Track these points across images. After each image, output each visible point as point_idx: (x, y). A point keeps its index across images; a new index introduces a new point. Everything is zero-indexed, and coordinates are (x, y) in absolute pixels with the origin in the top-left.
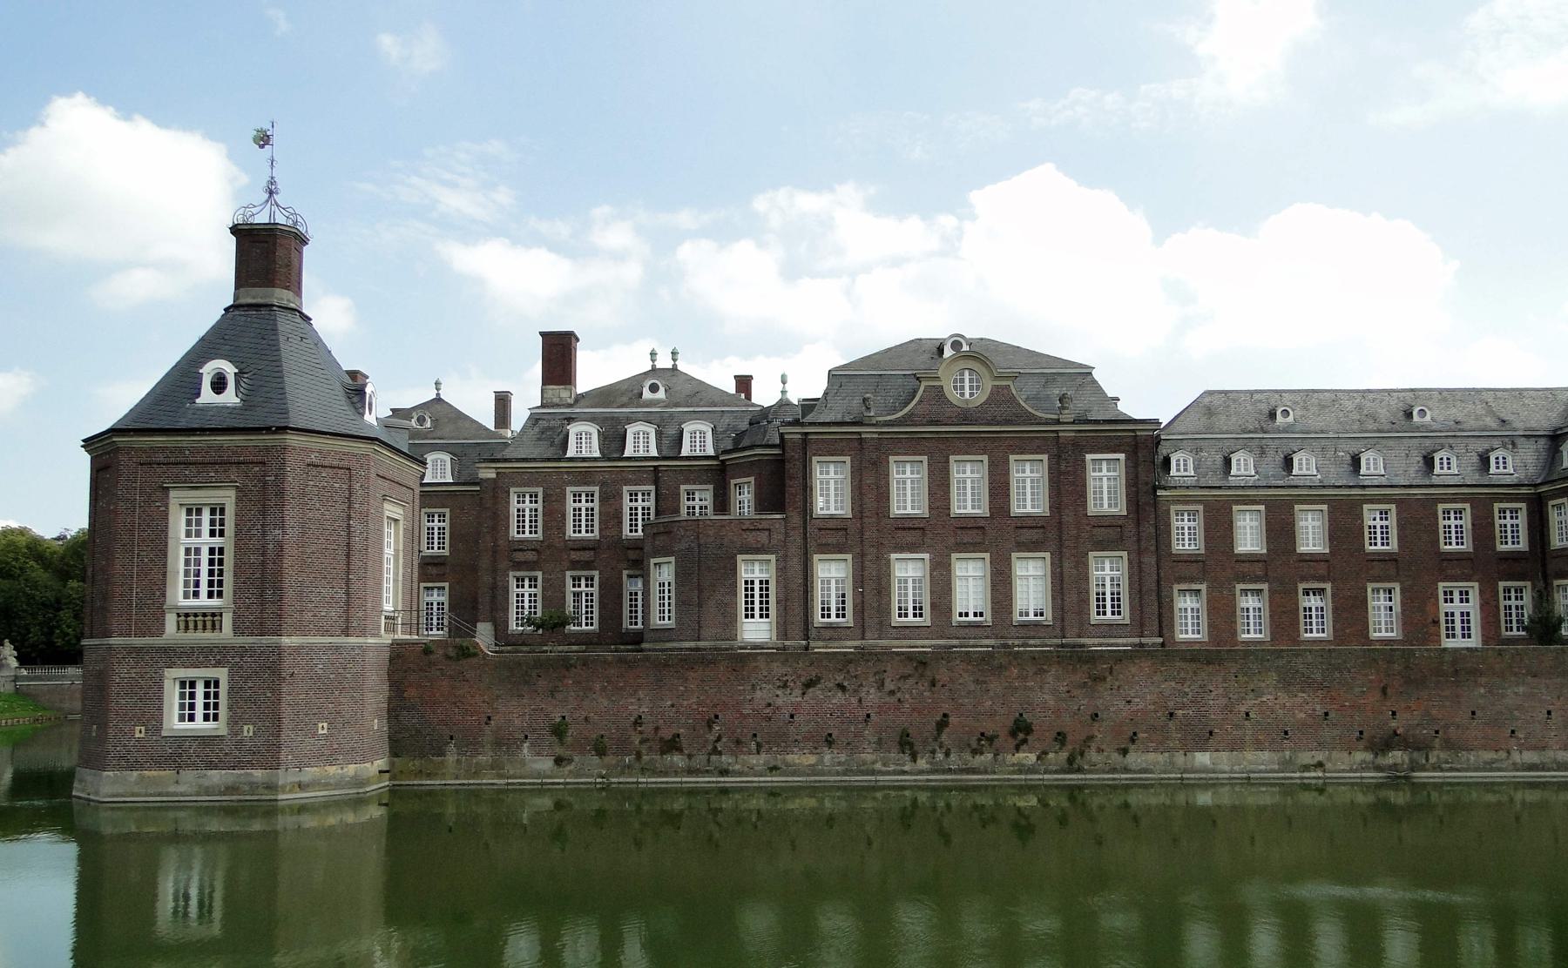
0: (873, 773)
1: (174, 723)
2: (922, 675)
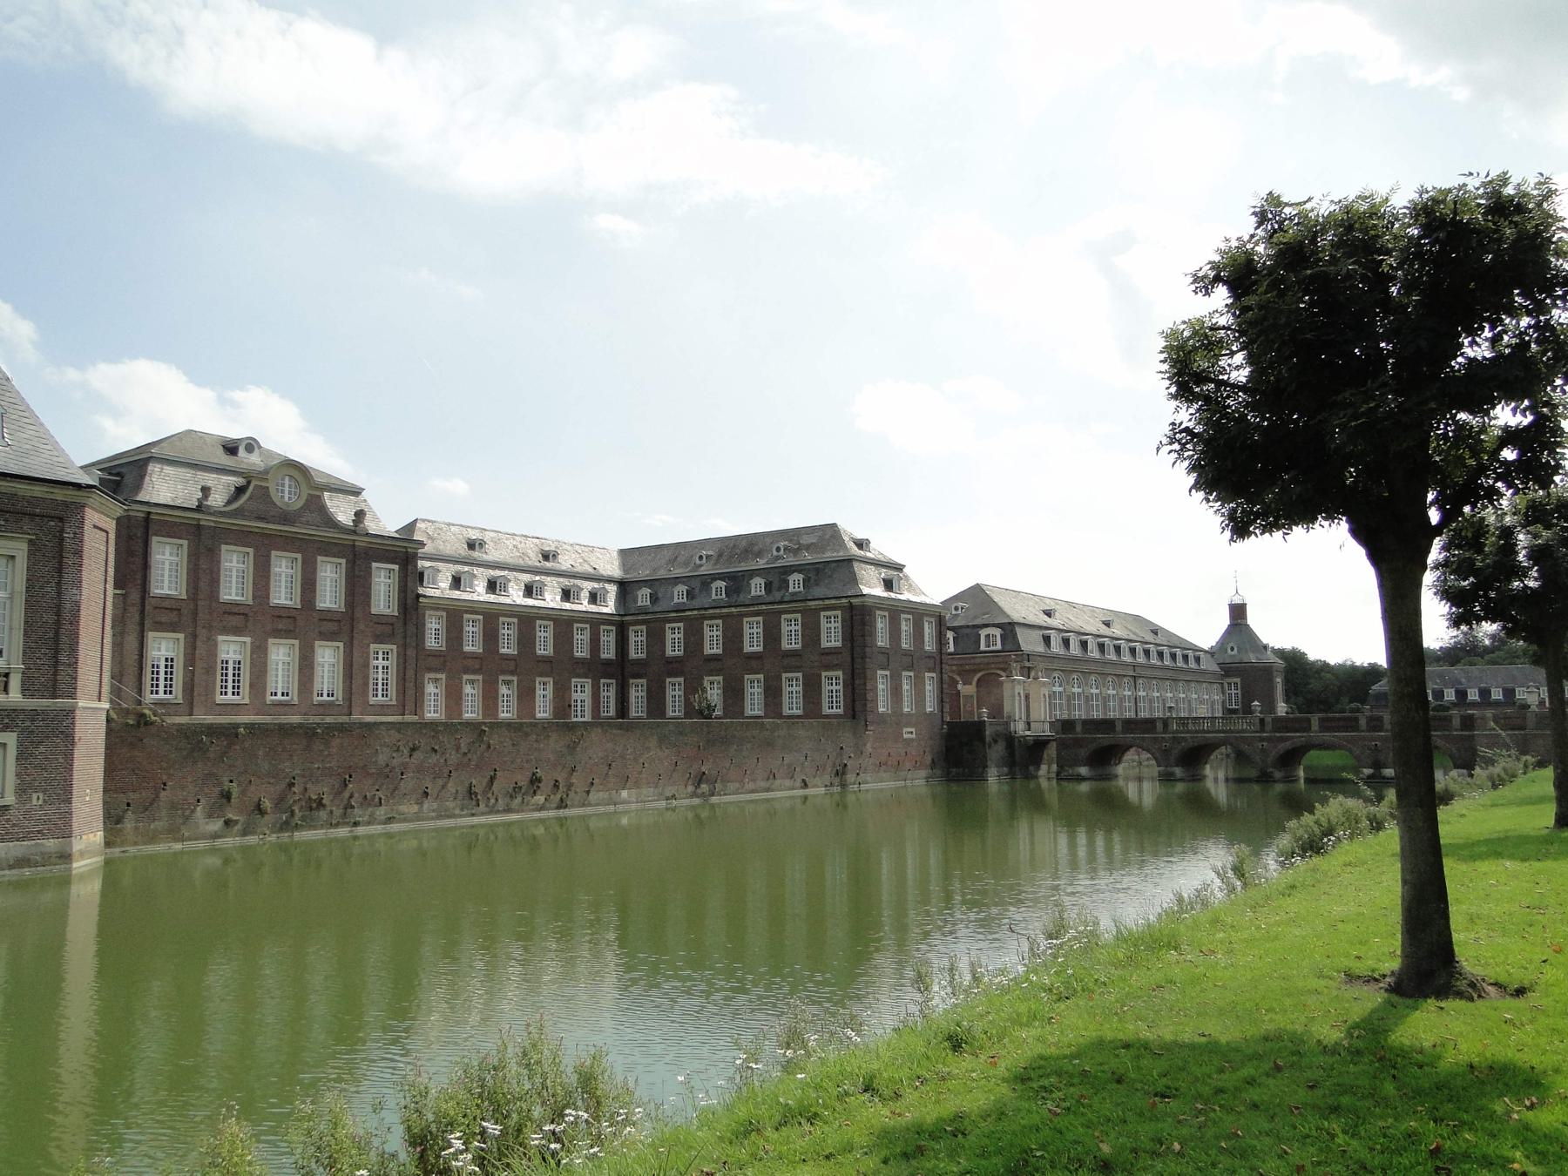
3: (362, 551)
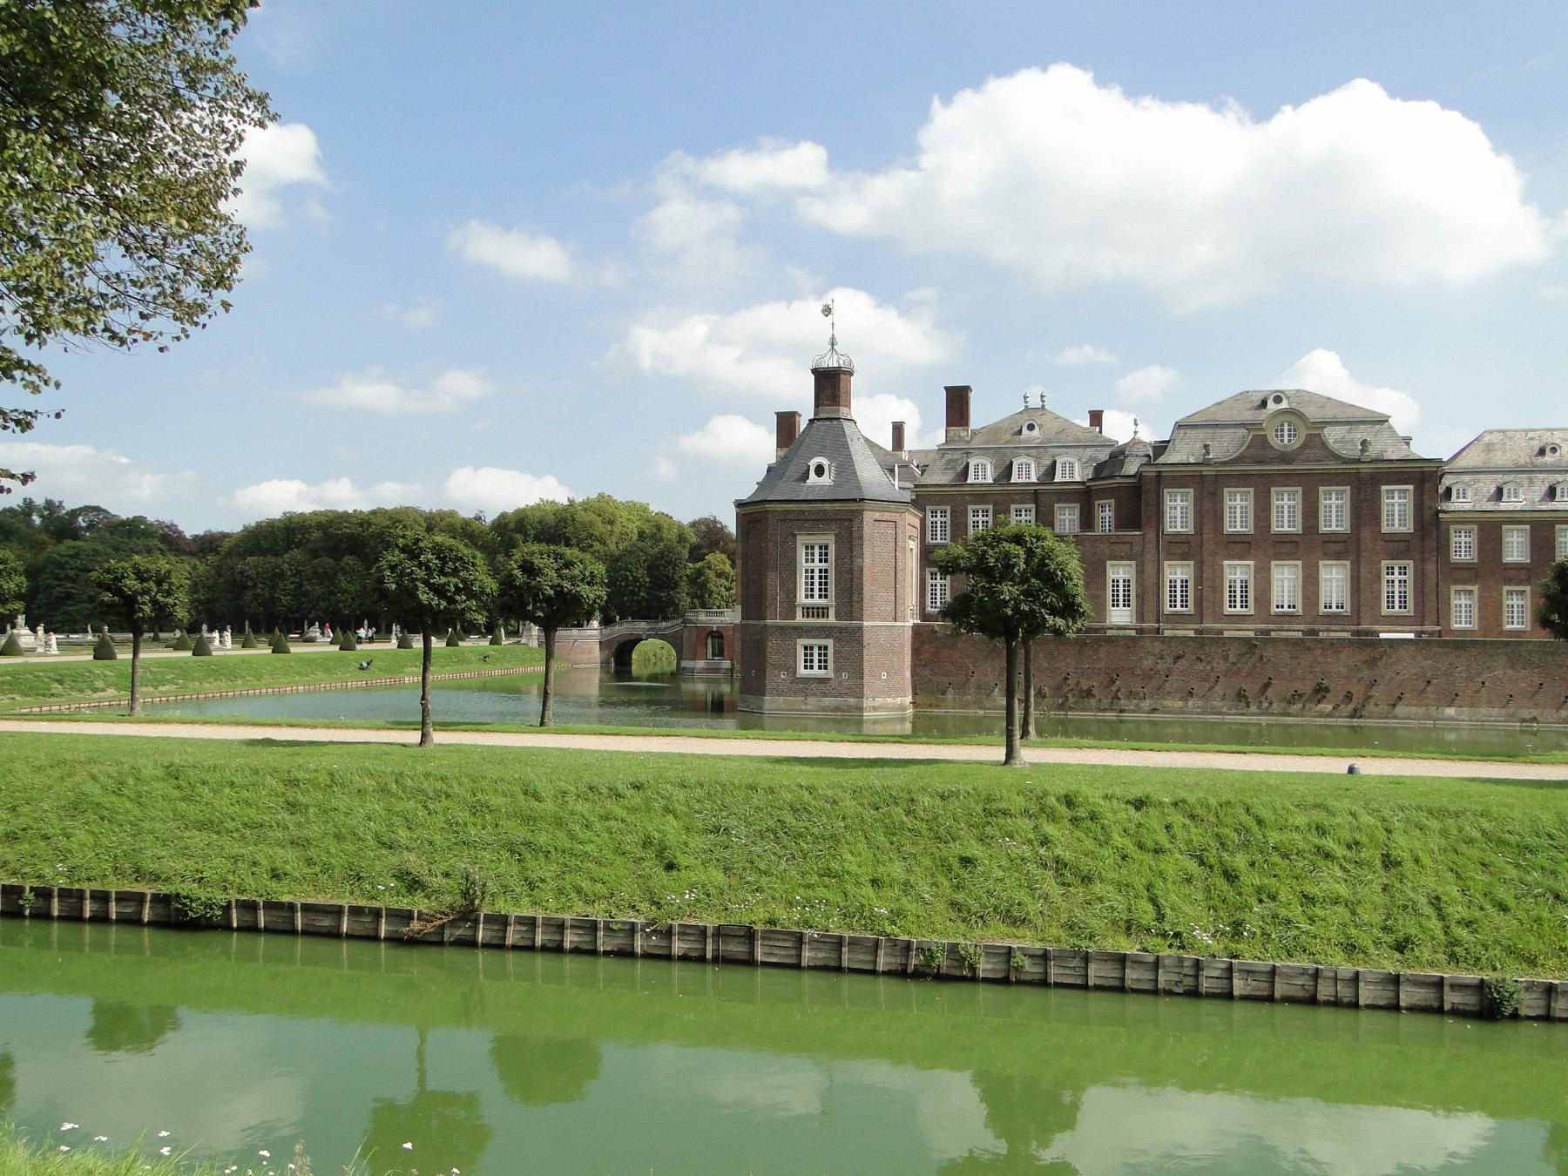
1: (802, 672)
3: (1367, 480)
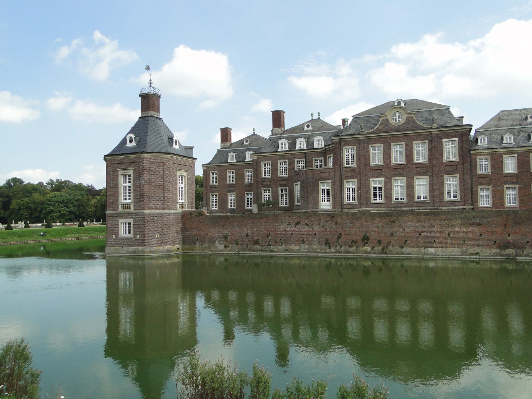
0: (317, 252)
1: (122, 234)
2: (333, 221)
